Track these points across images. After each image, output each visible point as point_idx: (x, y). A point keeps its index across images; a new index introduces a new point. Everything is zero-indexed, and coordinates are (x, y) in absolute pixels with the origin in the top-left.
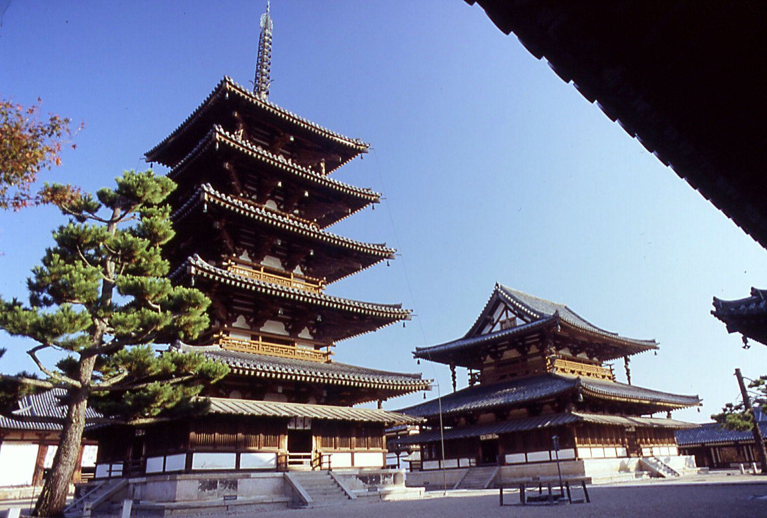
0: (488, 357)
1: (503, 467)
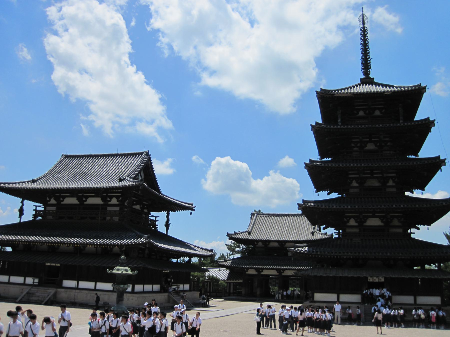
1: (59, 290)
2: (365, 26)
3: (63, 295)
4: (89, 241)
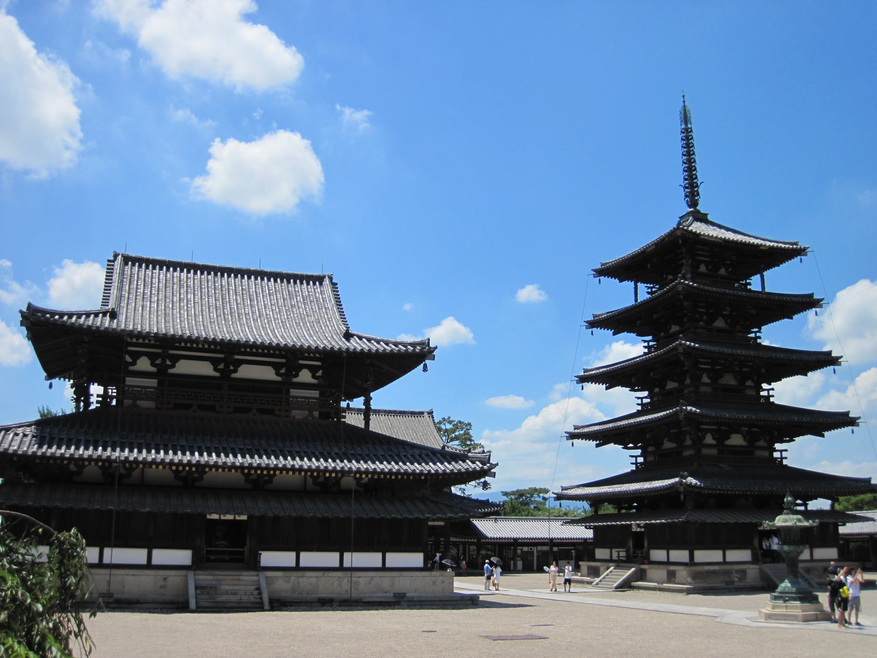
2: (689, 126)
3: (283, 585)
4: (346, 465)
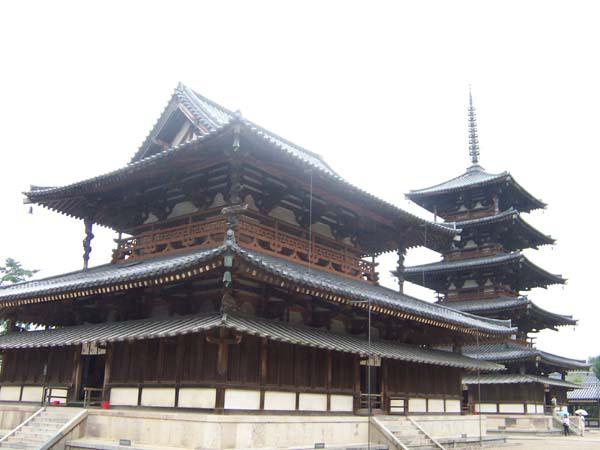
0: (151, 215)
